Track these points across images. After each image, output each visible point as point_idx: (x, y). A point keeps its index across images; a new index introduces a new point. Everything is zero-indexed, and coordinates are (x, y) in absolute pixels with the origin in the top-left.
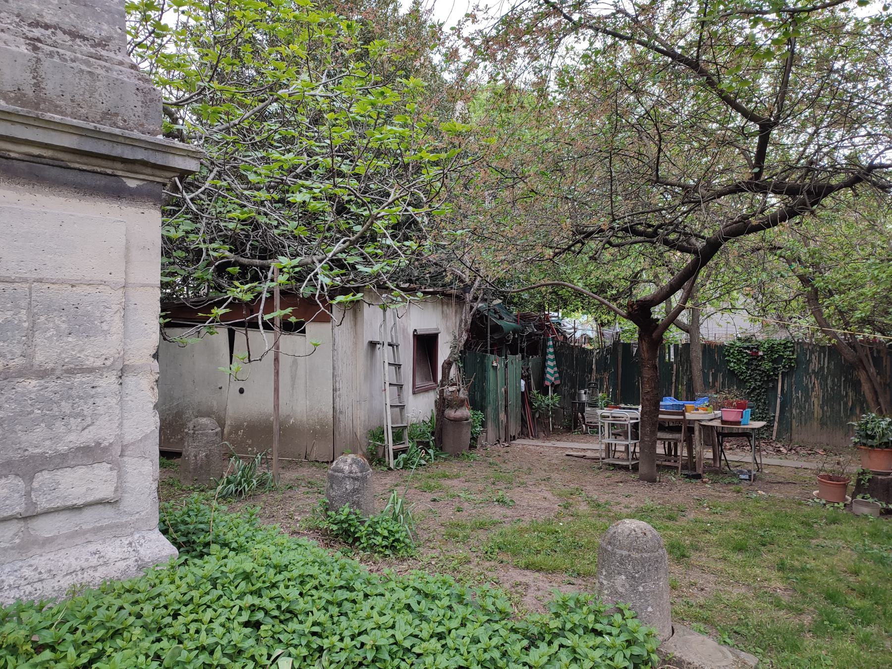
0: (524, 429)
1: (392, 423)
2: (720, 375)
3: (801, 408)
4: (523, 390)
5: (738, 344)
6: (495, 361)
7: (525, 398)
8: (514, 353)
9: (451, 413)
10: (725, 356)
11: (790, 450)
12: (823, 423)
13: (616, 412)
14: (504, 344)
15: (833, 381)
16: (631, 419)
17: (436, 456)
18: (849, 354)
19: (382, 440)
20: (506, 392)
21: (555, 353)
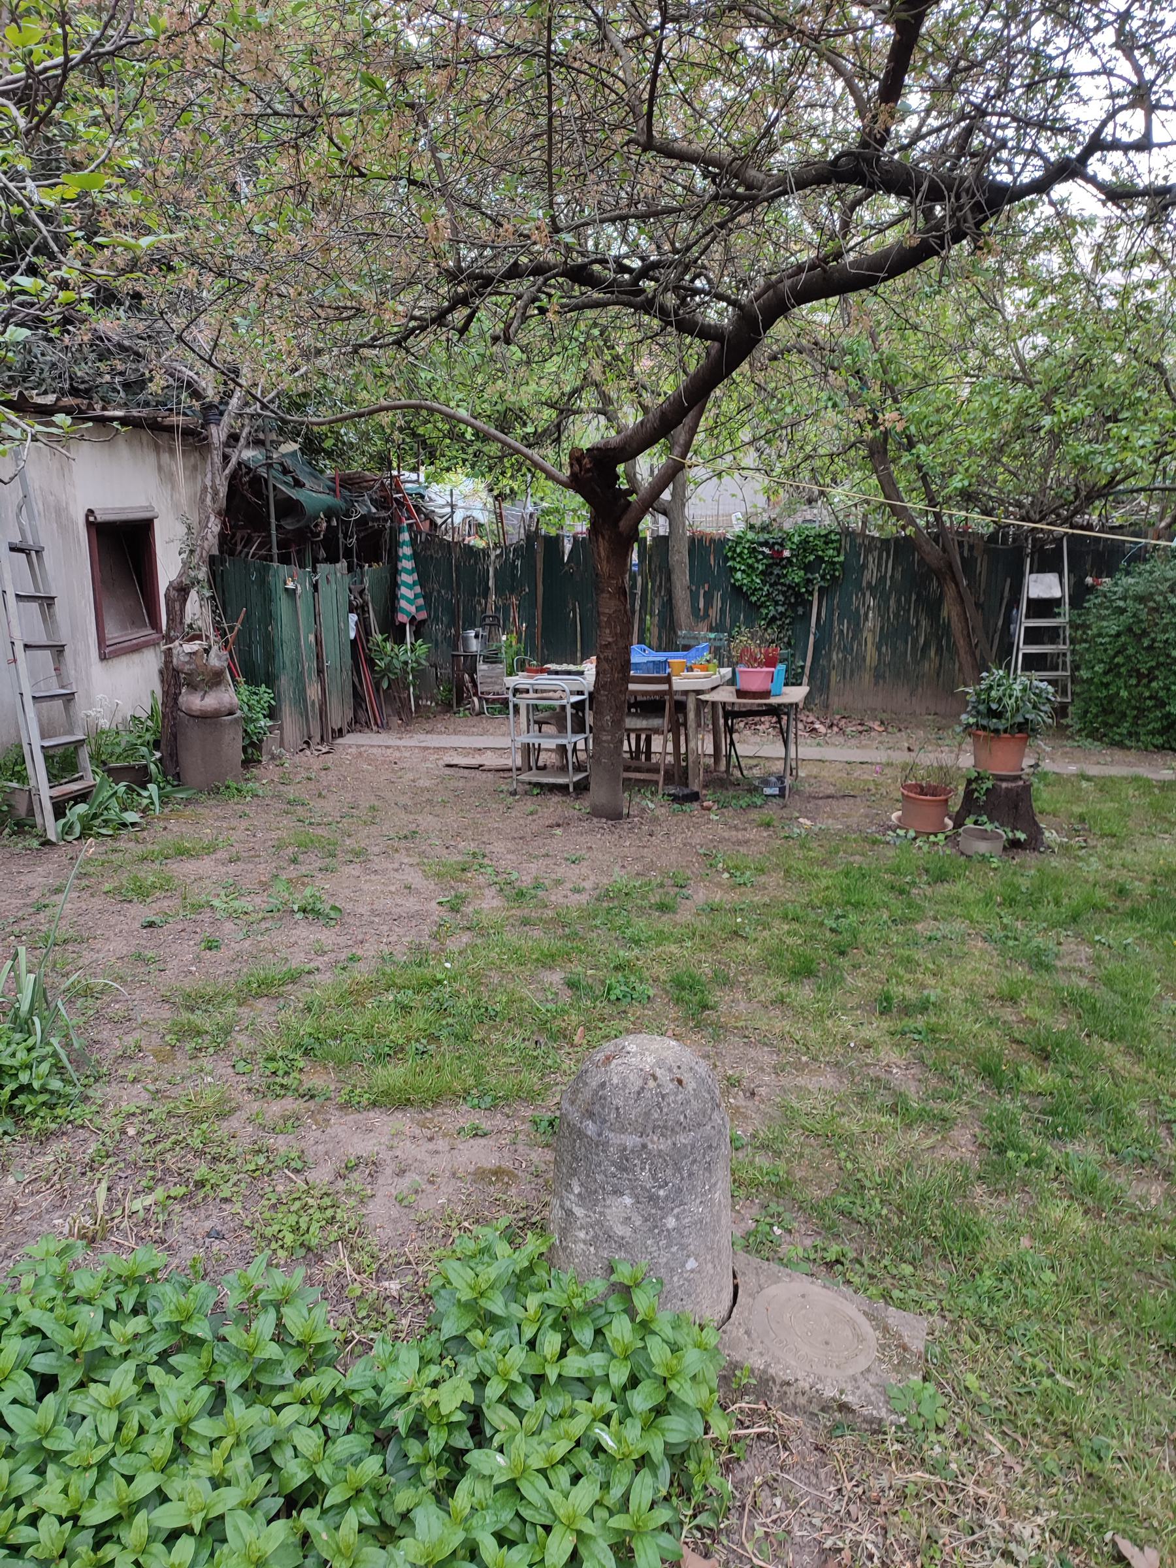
0: (360, 713)
1: (43, 737)
2: (718, 595)
3: (847, 650)
4: (352, 635)
5: (751, 535)
6: (290, 578)
7: (360, 653)
8: (332, 559)
9: (194, 701)
10: (726, 559)
11: (831, 726)
12: (878, 676)
13: (543, 680)
14: (308, 542)
15: (898, 601)
16: (572, 693)
17: (164, 800)
18: (933, 552)
19: (22, 778)
20: (318, 642)
21: (415, 556)
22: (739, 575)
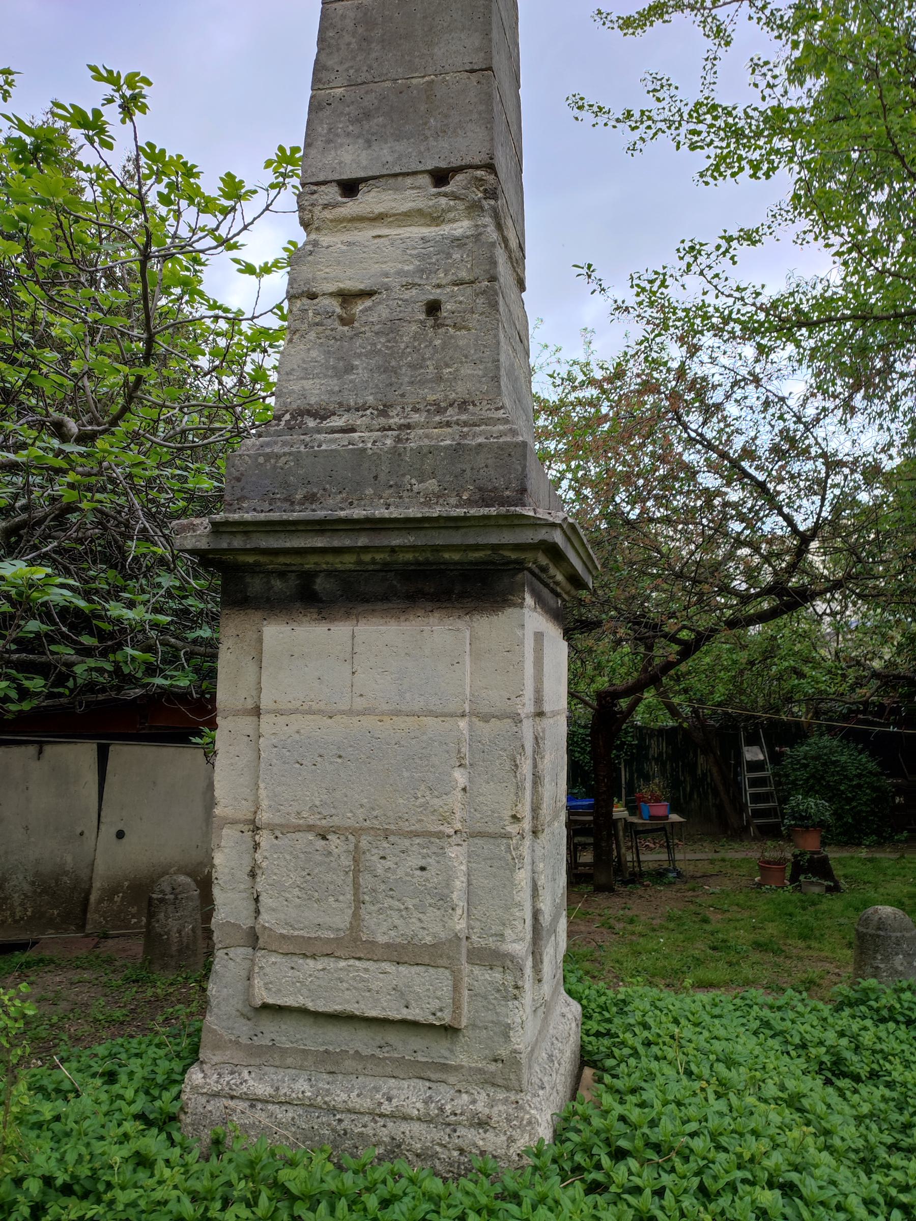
22: (577, 755)
